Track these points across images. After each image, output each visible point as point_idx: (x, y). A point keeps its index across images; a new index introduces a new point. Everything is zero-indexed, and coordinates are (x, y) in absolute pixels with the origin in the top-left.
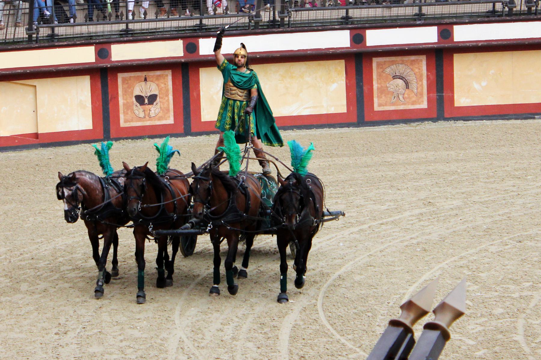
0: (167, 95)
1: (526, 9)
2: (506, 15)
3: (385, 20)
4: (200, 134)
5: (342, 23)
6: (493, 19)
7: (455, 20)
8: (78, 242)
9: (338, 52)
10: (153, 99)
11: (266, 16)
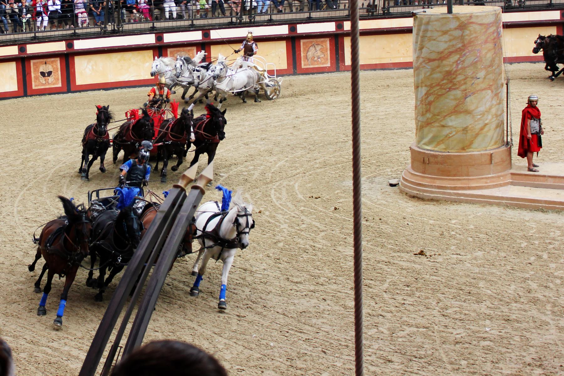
0: (57, 71)
1: (249, 20)
2: (238, 24)
3: (174, 28)
4: (76, 92)
5: (150, 30)
6: (231, 26)
7: (211, 27)
8: (11, 151)
9: (149, 46)
10: (50, 73)
11: (109, 27)
